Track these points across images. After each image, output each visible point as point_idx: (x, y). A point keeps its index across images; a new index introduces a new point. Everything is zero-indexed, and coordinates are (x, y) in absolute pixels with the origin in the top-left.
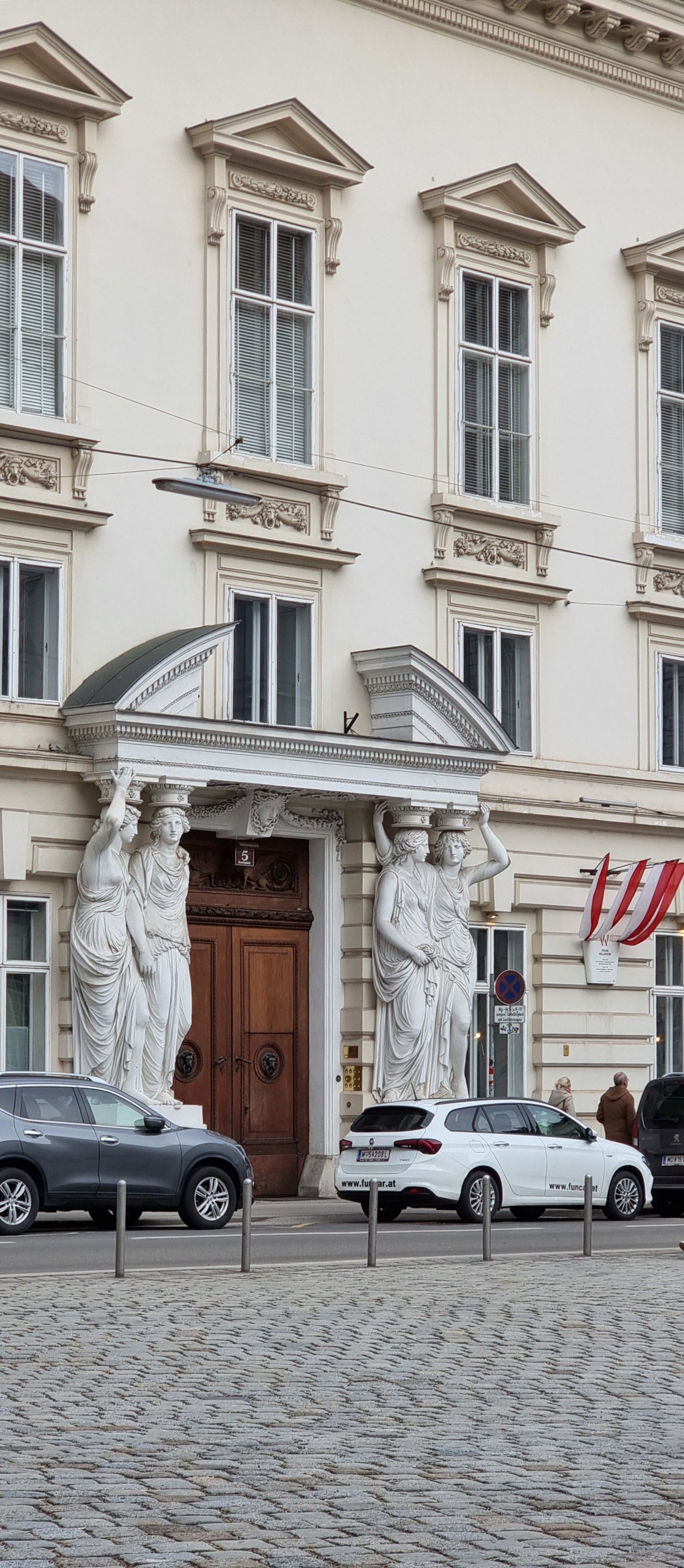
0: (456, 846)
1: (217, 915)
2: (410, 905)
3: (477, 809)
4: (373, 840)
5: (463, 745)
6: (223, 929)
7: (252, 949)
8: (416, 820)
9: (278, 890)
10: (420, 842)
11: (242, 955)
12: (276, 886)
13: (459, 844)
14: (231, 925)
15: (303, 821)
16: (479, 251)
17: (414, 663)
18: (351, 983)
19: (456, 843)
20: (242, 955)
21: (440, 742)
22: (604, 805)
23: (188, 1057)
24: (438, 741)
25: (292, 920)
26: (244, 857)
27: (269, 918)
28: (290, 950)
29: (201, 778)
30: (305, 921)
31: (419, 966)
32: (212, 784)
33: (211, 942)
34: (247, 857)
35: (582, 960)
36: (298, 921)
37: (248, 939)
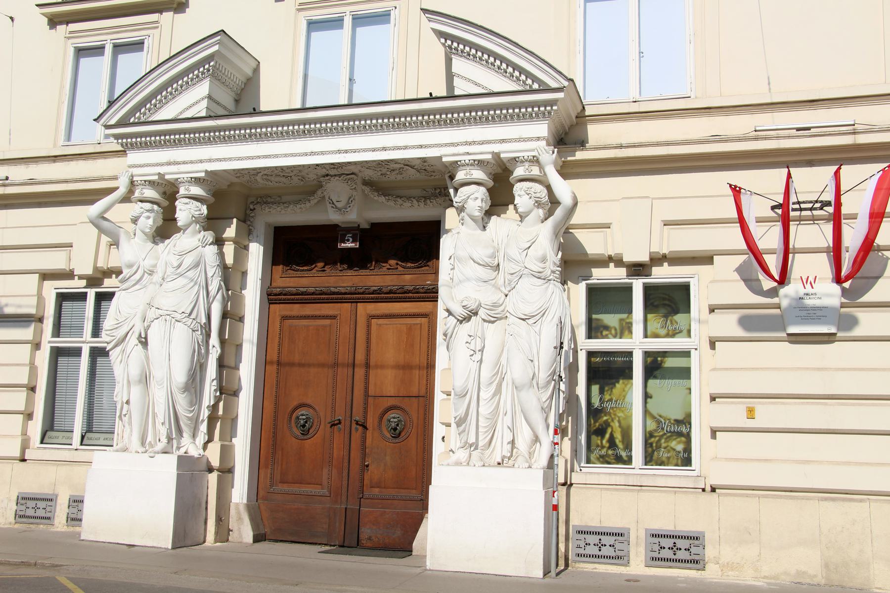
0: (519, 195)
1: (334, 293)
3: (534, 154)
6: (347, 306)
7: (381, 321)
11: (369, 326)
13: (523, 193)
15: (400, 201)
19: (519, 193)
20: (369, 326)
25: (417, 293)
27: (390, 292)
28: (424, 320)
29: (199, 170)
31: (461, 322)
33: (333, 317)
37: (374, 313)
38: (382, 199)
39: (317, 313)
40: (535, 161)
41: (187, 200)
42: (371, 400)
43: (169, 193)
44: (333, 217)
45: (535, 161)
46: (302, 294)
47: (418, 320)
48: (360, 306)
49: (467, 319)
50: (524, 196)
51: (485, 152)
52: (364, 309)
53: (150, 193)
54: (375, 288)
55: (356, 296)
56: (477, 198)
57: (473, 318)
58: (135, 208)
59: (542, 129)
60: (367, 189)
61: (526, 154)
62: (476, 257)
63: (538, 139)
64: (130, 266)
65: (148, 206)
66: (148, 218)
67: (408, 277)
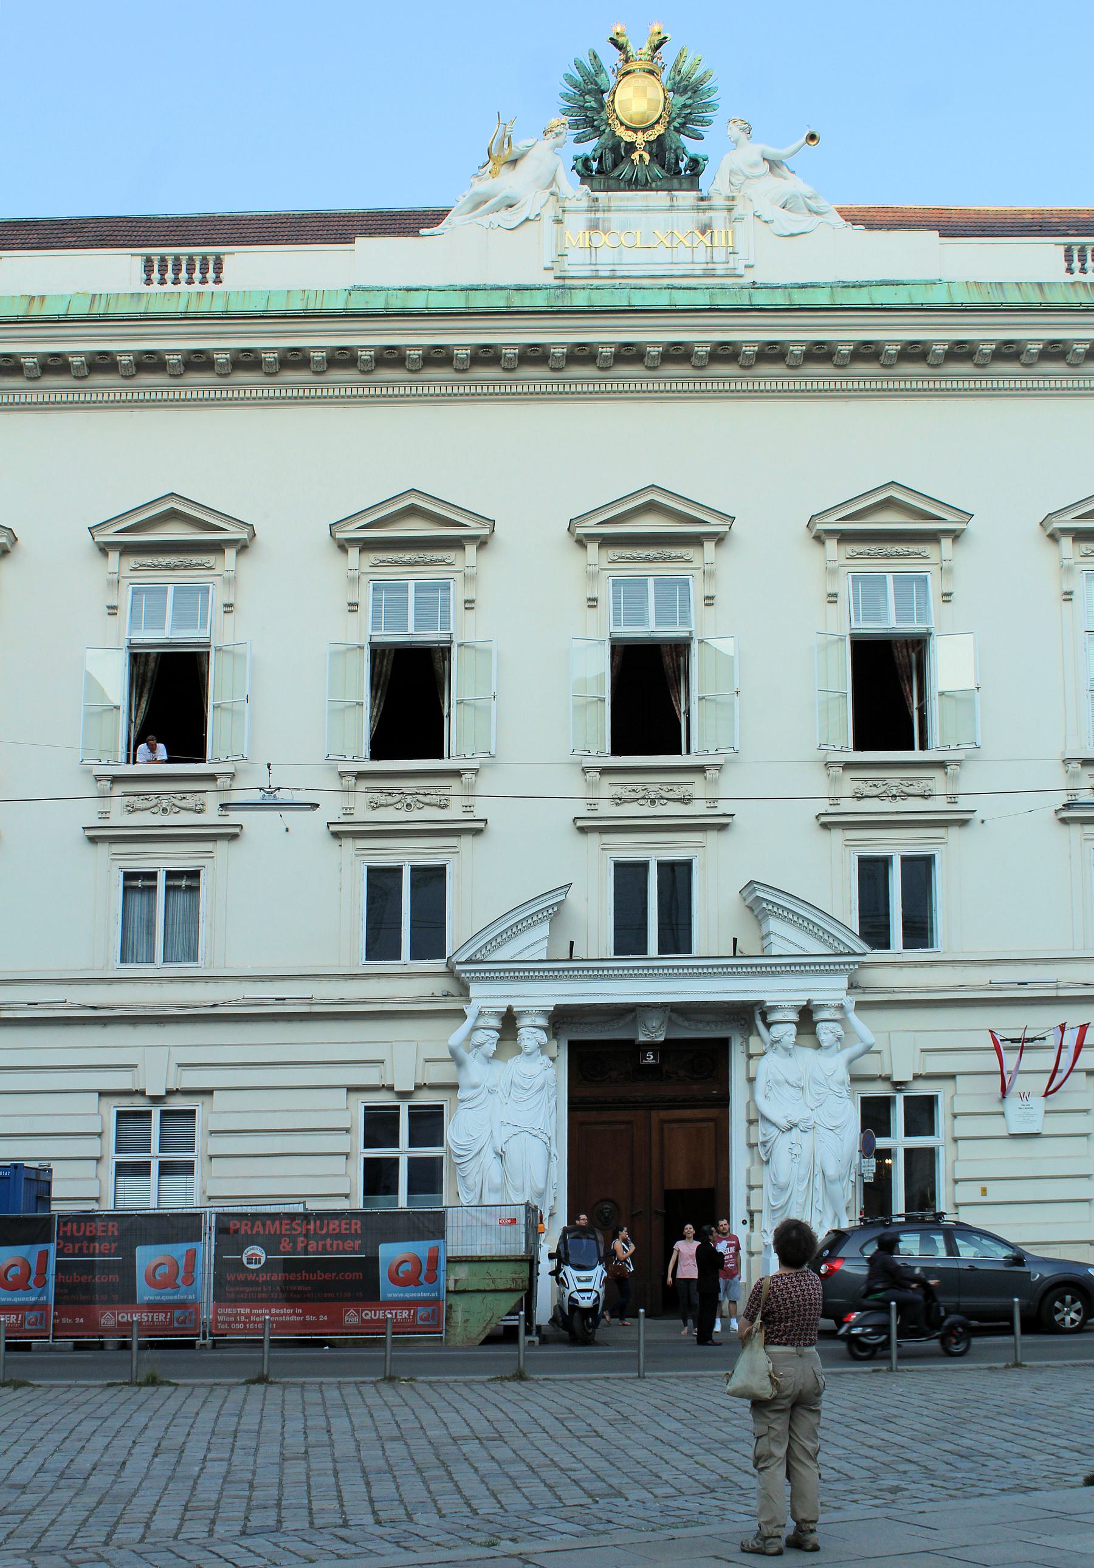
2: (777, 1083)
4: (759, 1035)
10: (787, 1032)
11: (662, 1130)
14: (651, 1108)
16: (870, 556)
17: (758, 894)
18: (751, 1146)
22: (1019, 984)
27: (684, 1101)
28: (711, 1124)
29: (550, 1003)
30: (724, 1101)
32: (557, 1007)
35: (1003, 1114)
38: (686, 1024)
40: (841, 1007)
41: (534, 1030)
43: (509, 1022)
44: (642, 1038)
45: (841, 1007)
47: (705, 1124)
48: (654, 1113)
50: (826, 1032)
51: (801, 999)
52: (657, 1115)
59: (843, 982)
60: (674, 1016)
61: (833, 1003)
63: (839, 989)
64: (475, 1087)
67: (695, 1087)
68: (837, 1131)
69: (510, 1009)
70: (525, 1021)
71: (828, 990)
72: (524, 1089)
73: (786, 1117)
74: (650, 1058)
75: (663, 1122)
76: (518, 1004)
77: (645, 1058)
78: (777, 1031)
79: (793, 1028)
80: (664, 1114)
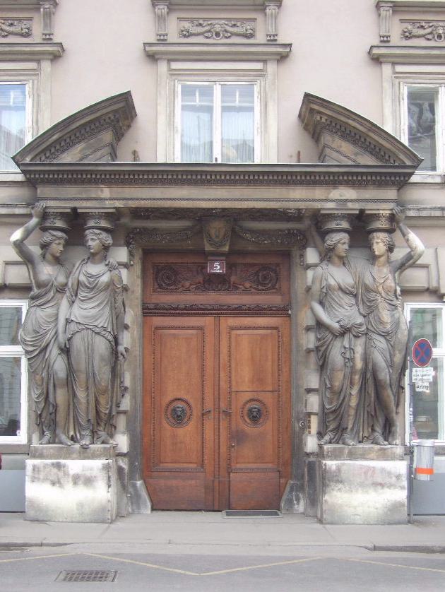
5: (375, 164)
8: (333, 225)
9: (263, 290)
10: (340, 240)
12: (260, 287)
21: (353, 164)
23: (178, 409)
24: (350, 163)
26: (216, 267)
31: (337, 336)
33: (201, 328)
34: (219, 267)
36: (277, 310)
39: (186, 325)
42: (233, 394)
46: (174, 309)
48: (222, 320)
49: (342, 334)
51: (354, 208)
53: (59, 224)
54: (236, 306)
55: (219, 311)
56: (344, 243)
57: (347, 337)
58: (47, 237)
62: (343, 287)
65: (60, 234)
66: (59, 244)
68: (388, 338)
69: (74, 209)
70: (91, 223)
71: (380, 201)
72: (88, 288)
73: (338, 322)
74: (217, 268)
75: (232, 328)
76: (83, 206)
77: (212, 267)
78: (334, 239)
79: (344, 237)
80: (232, 321)
